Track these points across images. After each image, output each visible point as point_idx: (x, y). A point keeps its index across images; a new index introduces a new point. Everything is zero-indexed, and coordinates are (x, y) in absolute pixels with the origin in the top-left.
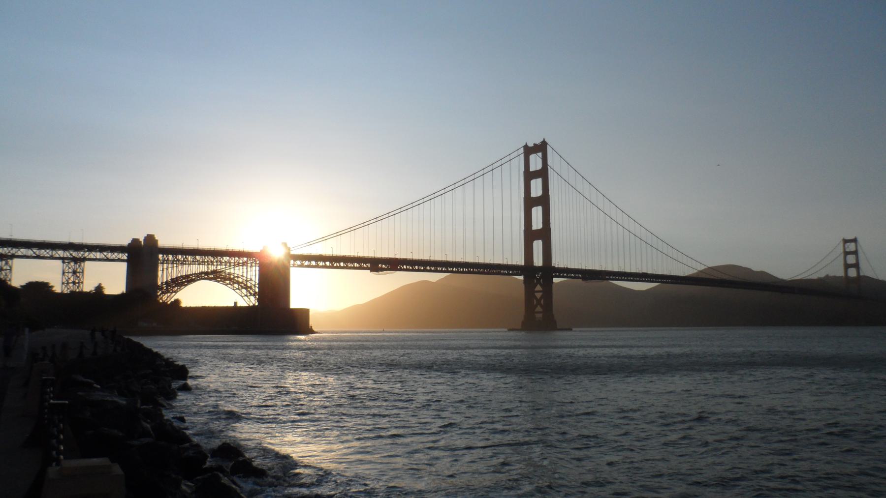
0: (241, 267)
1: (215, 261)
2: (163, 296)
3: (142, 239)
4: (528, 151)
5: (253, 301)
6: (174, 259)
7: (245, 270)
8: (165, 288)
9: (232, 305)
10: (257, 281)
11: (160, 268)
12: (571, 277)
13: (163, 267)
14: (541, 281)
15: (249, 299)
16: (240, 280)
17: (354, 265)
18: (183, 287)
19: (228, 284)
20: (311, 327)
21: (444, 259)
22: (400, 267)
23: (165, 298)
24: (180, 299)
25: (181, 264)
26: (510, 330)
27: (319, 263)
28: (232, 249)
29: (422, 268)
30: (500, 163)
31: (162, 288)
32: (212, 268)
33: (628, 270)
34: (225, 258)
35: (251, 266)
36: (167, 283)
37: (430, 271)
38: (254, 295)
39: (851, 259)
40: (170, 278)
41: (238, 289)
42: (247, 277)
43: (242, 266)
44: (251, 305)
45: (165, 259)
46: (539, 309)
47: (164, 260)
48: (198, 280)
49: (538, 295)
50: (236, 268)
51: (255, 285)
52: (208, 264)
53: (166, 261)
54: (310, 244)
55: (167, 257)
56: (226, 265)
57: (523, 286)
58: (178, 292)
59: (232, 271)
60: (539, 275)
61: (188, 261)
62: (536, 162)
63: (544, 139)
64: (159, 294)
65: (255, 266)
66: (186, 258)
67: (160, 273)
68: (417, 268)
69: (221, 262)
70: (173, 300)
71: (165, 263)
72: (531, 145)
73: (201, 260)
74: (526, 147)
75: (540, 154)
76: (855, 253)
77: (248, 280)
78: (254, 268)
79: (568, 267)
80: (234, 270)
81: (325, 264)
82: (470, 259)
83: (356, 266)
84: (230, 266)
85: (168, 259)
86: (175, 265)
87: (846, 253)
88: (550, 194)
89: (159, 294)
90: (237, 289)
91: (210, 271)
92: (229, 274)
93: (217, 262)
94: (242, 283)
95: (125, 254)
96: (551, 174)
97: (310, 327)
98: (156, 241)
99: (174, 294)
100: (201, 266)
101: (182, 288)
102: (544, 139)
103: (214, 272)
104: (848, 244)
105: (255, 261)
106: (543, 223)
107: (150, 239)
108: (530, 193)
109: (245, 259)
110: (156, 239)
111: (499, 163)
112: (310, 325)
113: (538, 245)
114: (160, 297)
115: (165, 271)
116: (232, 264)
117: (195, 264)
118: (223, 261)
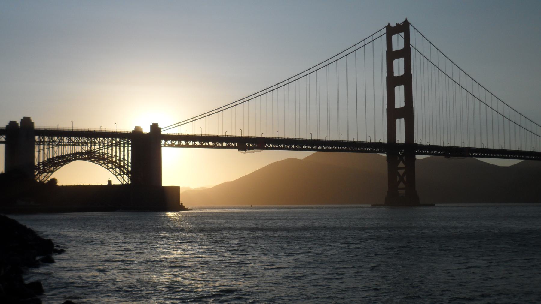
0: (114, 148)
1: (89, 142)
2: (40, 176)
3: (18, 122)
4: (391, 31)
5: (126, 179)
6: (50, 140)
7: (118, 150)
8: (42, 168)
9: (106, 183)
10: (130, 161)
11: (37, 149)
12: (433, 154)
13: (39, 148)
14: (404, 158)
15: (123, 178)
16: (114, 160)
17: (222, 144)
18: (59, 167)
19: (102, 164)
20: (182, 204)
21: (309, 137)
22: (267, 146)
23: (41, 178)
24: (56, 178)
25: (56, 145)
26: (373, 206)
27: (189, 142)
28: (105, 130)
29: (288, 147)
30: (363, 44)
31: (39, 168)
32: (87, 148)
33: (490, 147)
34: (98, 139)
35: (124, 146)
36: (43, 163)
37: (296, 149)
38: (127, 174)
40: (46, 159)
41: (112, 168)
42: (120, 157)
43: (116, 146)
44: (124, 183)
45: (41, 140)
46: (402, 185)
47: (40, 141)
48: (73, 160)
49: (401, 172)
50: (110, 149)
51: (128, 166)
52: (83, 145)
53: (42, 142)
54: (180, 124)
55: (43, 138)
56: (99, 146)
57: (386, 163)
58: (54, 171)
59: (106, 151)
60: (402, 153)
61: (63, 142)
62: (398, 42)
63: (406, 19)
64: (36, 174)
65: (128, 146)
66: (61, 139)
67: (36, 154)
69: (95, 143)
70: (49, 179)
71: (42, 144)
72: (393, 25)
73: (76, 141)
74: (388, 27)
75: (402, 34)
77: (121, 159)
78: (126, 148)
79: (431, 144)
80: (108, 150)
81: (195, 143)
82: (334, 137)
83: (224, 145)
84: (104, 146)
85: (44, 140)
86: (51, 146)
88: (412, 73)
89: (36, 174)
90: (111, 168)
91: (84, 151)
92: (104, 154)
93: (91, 142)
94: (116, 162)
95: (3, 137)
96: (414, 54)
97: (181, 204)
98: (33, 123)
99: (50, 173)
100: (76, 147)
101: (58, 168)
102: (406, 19)
103: (88, 152)
105: (128, 142)
106: (405, 102)
107: (27, 121)
108: (393, 73)
109: (118, 140)
110: (32, 121)
111: (362, 44)
112: (180, 202)
113: (400, 123)
114: (37, 177)
115: (41, 152)
116: (106, 145)
117: (70, 145)
118: (97, 142)
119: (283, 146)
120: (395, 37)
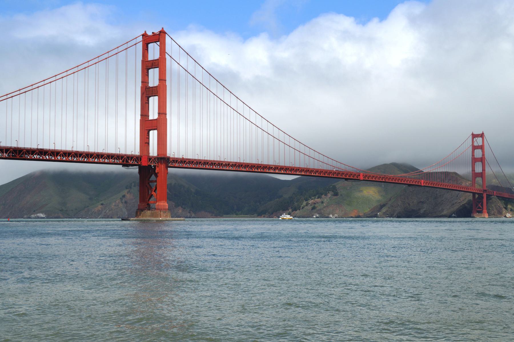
39: (478, 153)
68: (59, 159)
72: (149, 33)
74: (144, 35)
75: (158, 43)
76: (482, 147)
87: (474, 148)
104: (476, 138)
106: (159, 114)
119: (59, 158)
120: (151, 46)
